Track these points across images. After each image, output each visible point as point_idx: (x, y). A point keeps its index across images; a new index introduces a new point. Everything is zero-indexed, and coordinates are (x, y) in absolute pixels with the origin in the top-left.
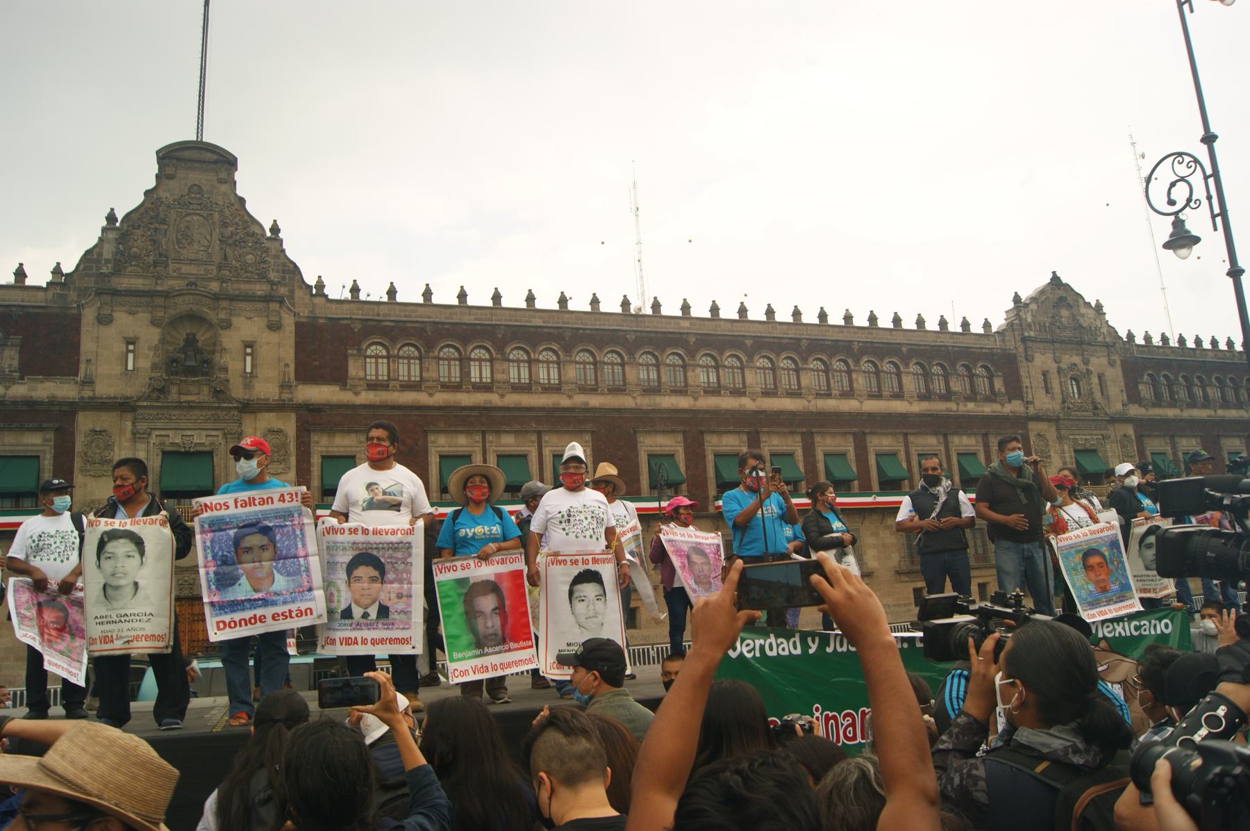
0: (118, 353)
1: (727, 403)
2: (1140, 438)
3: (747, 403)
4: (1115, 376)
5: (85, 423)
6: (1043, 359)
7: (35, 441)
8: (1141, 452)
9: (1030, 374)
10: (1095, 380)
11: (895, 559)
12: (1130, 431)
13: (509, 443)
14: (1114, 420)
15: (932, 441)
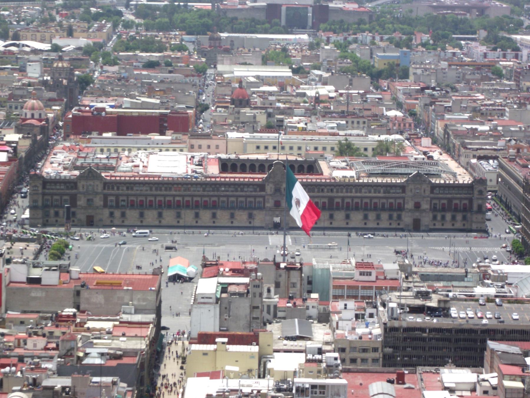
0: (269, 188)
1: (349, 194)
2: (431, 201)
3: (352, 195)
4: (428, 189)
5: (266, 197)
6: (411, 186)
7: (261, 199)
8: (431, 203)
9: (408, 189)
10: (423, 190)
11: (374, 218)
12: (429, 199)
13: (316, 200)
14: (424, 197)
15: (384, 201)
